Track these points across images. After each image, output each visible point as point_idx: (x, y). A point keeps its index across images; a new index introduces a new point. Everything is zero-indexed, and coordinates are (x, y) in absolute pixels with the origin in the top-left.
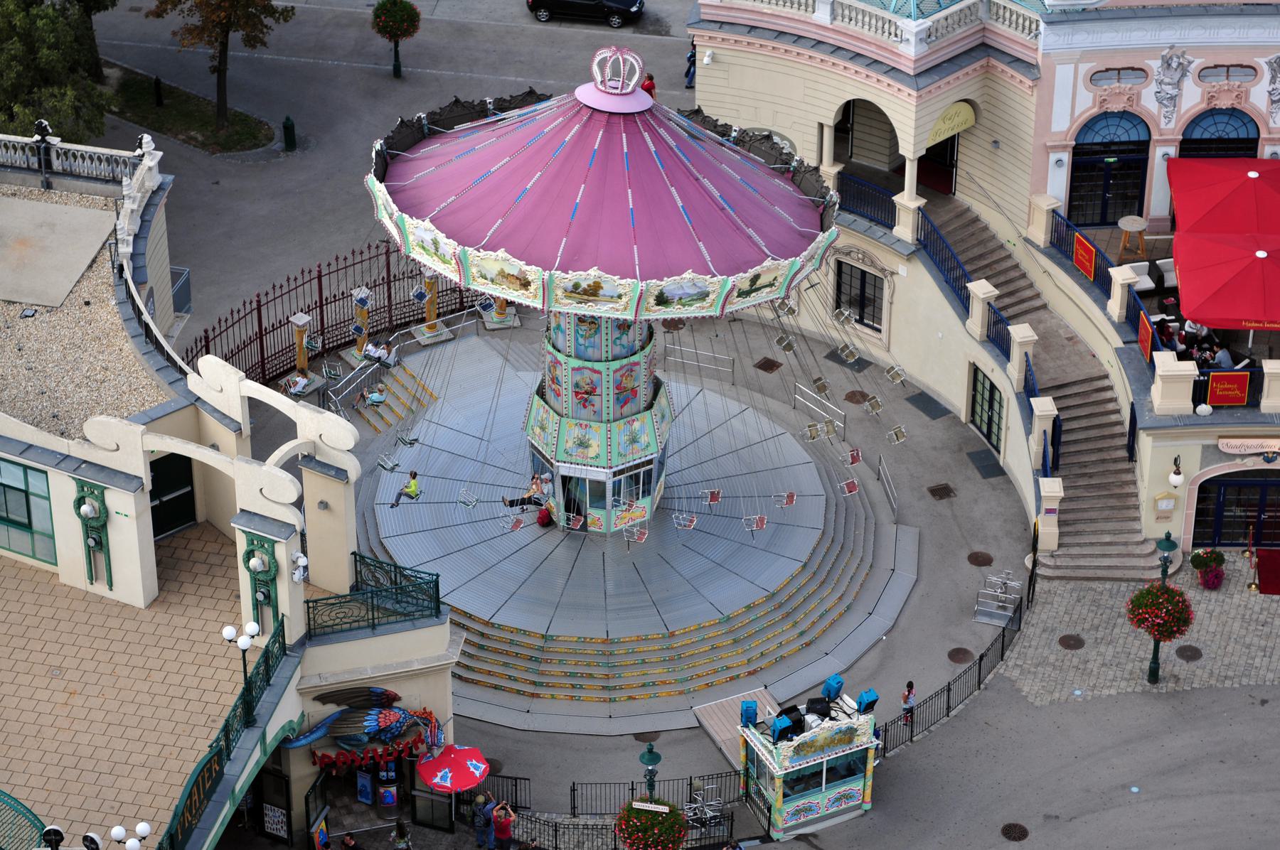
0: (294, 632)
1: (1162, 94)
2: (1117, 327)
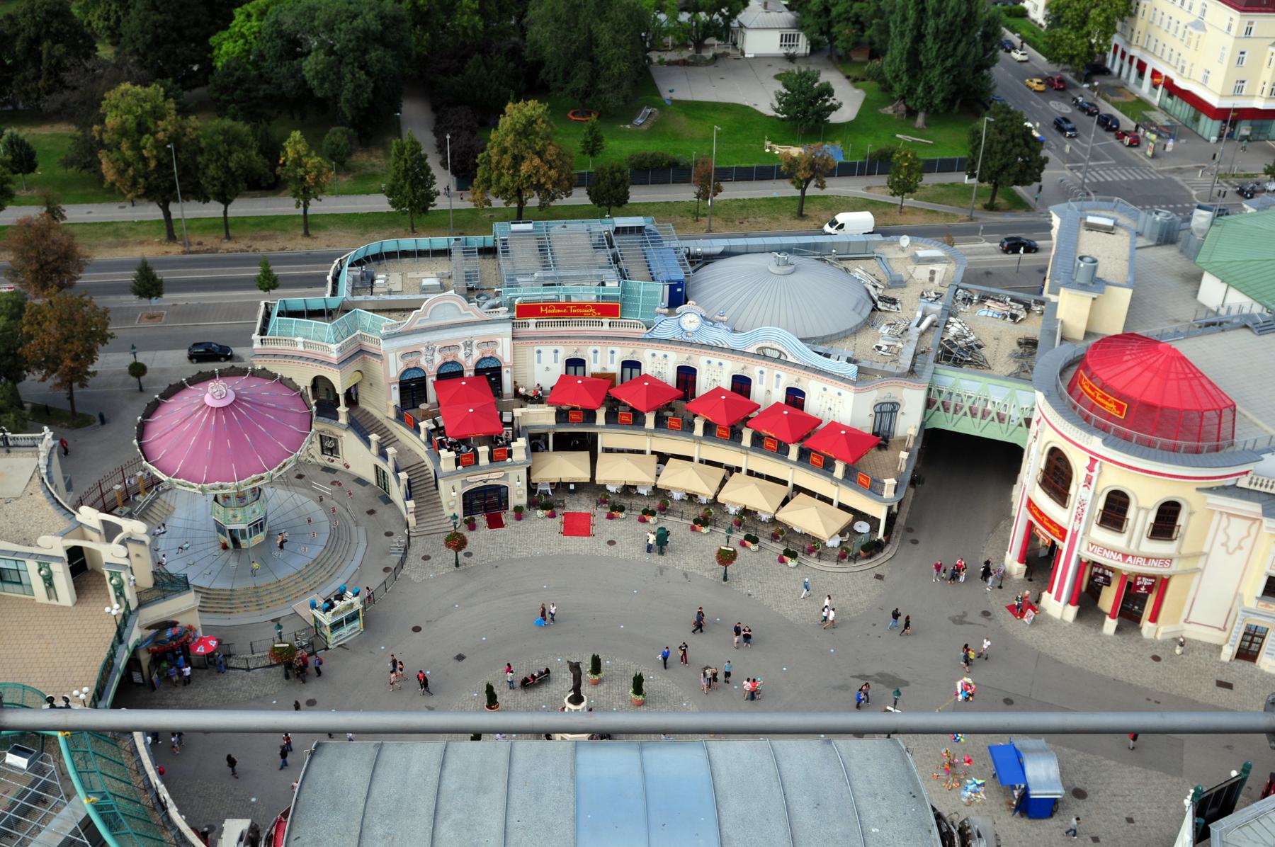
0: (133, 606)
2: (425, 443)
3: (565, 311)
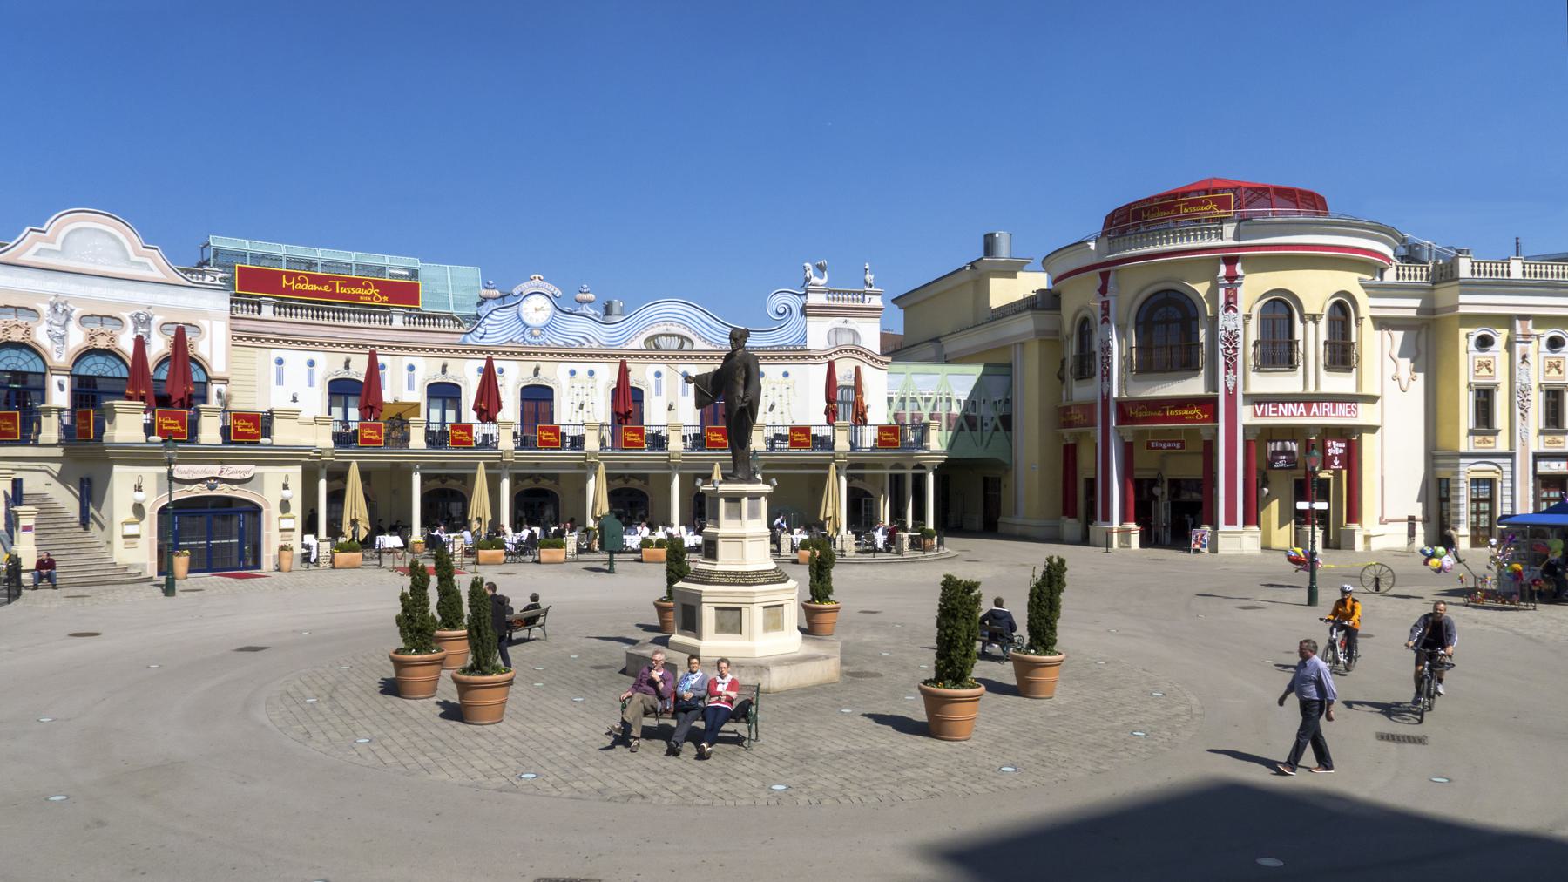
1: (53, 333)
3: (326, 289)
